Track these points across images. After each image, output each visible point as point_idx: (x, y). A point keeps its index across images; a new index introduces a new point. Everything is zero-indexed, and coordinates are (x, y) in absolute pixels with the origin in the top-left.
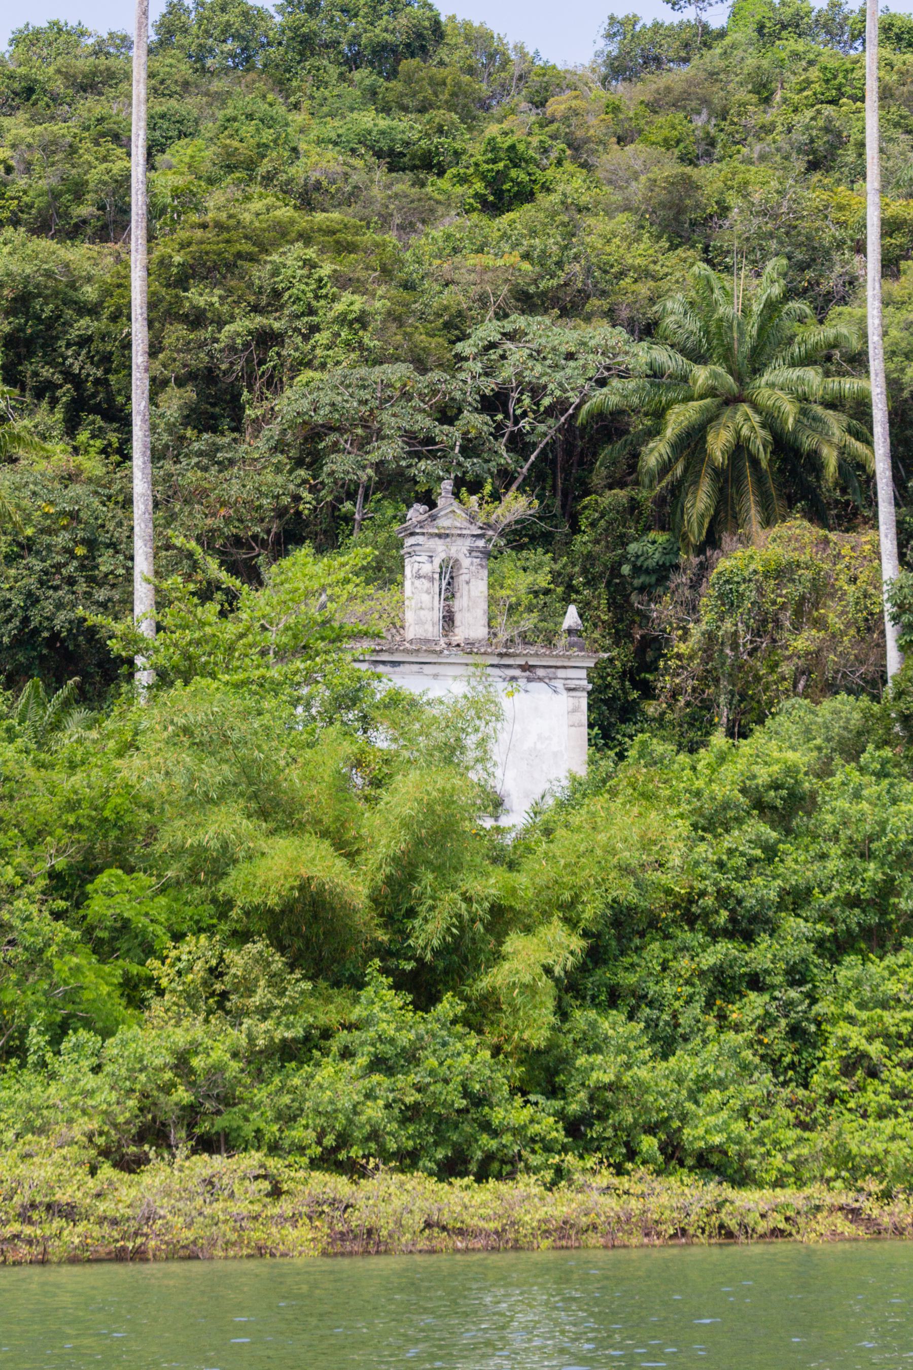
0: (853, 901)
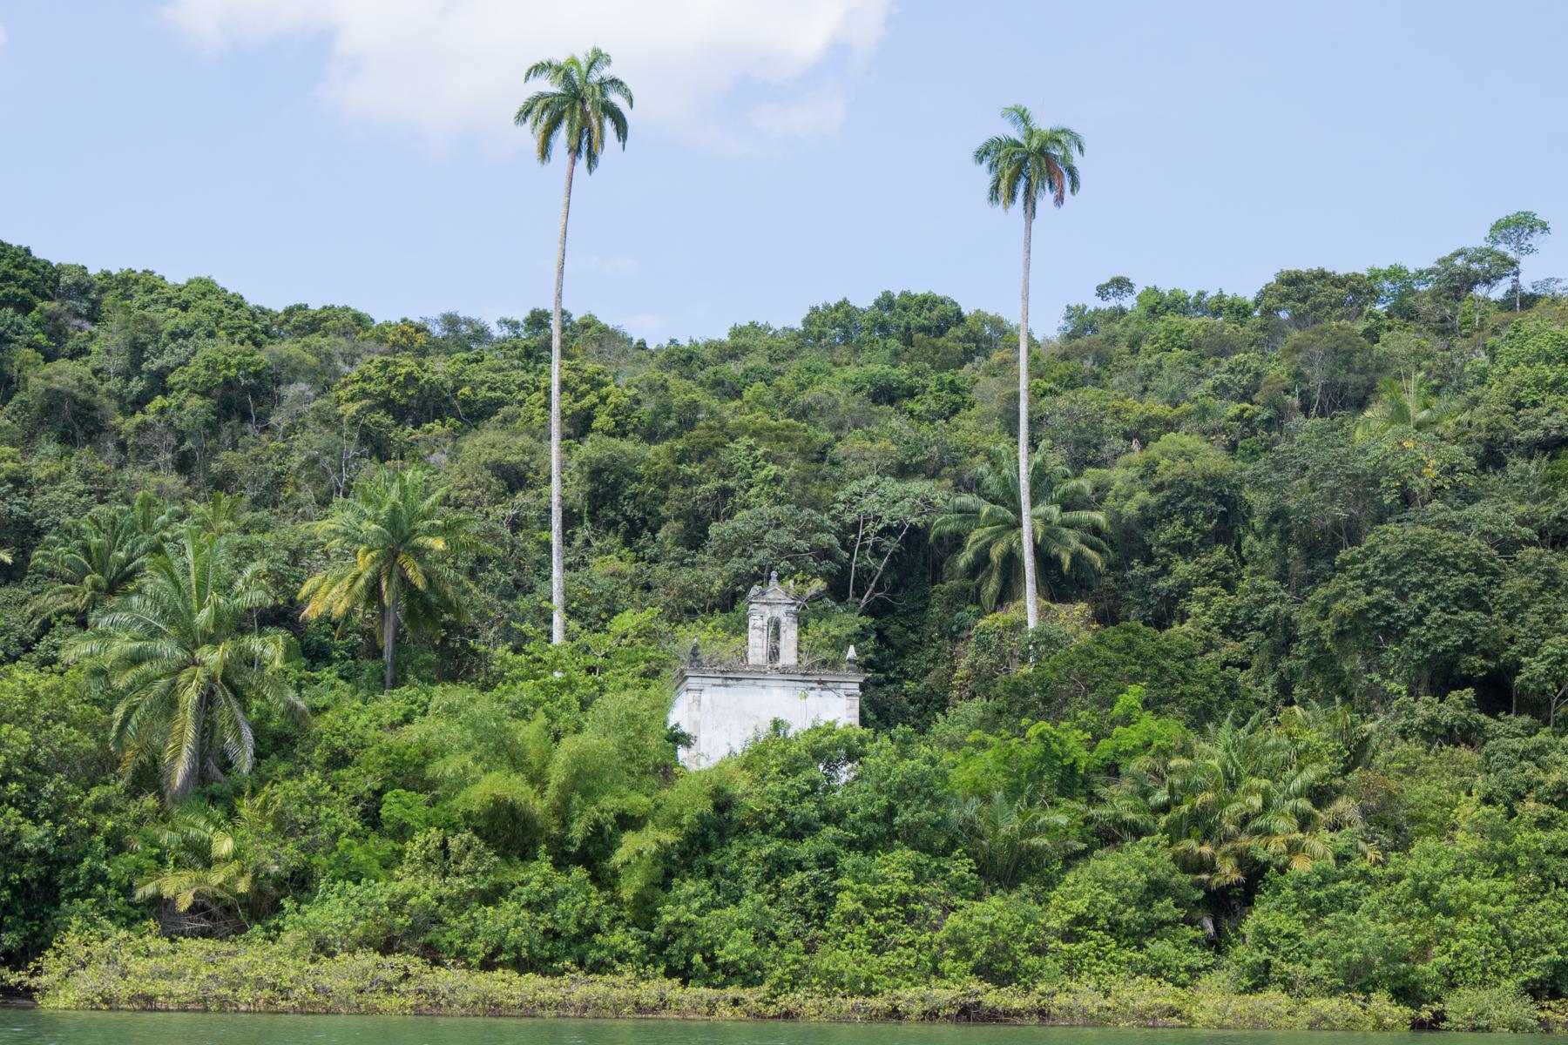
0: (872, 818)
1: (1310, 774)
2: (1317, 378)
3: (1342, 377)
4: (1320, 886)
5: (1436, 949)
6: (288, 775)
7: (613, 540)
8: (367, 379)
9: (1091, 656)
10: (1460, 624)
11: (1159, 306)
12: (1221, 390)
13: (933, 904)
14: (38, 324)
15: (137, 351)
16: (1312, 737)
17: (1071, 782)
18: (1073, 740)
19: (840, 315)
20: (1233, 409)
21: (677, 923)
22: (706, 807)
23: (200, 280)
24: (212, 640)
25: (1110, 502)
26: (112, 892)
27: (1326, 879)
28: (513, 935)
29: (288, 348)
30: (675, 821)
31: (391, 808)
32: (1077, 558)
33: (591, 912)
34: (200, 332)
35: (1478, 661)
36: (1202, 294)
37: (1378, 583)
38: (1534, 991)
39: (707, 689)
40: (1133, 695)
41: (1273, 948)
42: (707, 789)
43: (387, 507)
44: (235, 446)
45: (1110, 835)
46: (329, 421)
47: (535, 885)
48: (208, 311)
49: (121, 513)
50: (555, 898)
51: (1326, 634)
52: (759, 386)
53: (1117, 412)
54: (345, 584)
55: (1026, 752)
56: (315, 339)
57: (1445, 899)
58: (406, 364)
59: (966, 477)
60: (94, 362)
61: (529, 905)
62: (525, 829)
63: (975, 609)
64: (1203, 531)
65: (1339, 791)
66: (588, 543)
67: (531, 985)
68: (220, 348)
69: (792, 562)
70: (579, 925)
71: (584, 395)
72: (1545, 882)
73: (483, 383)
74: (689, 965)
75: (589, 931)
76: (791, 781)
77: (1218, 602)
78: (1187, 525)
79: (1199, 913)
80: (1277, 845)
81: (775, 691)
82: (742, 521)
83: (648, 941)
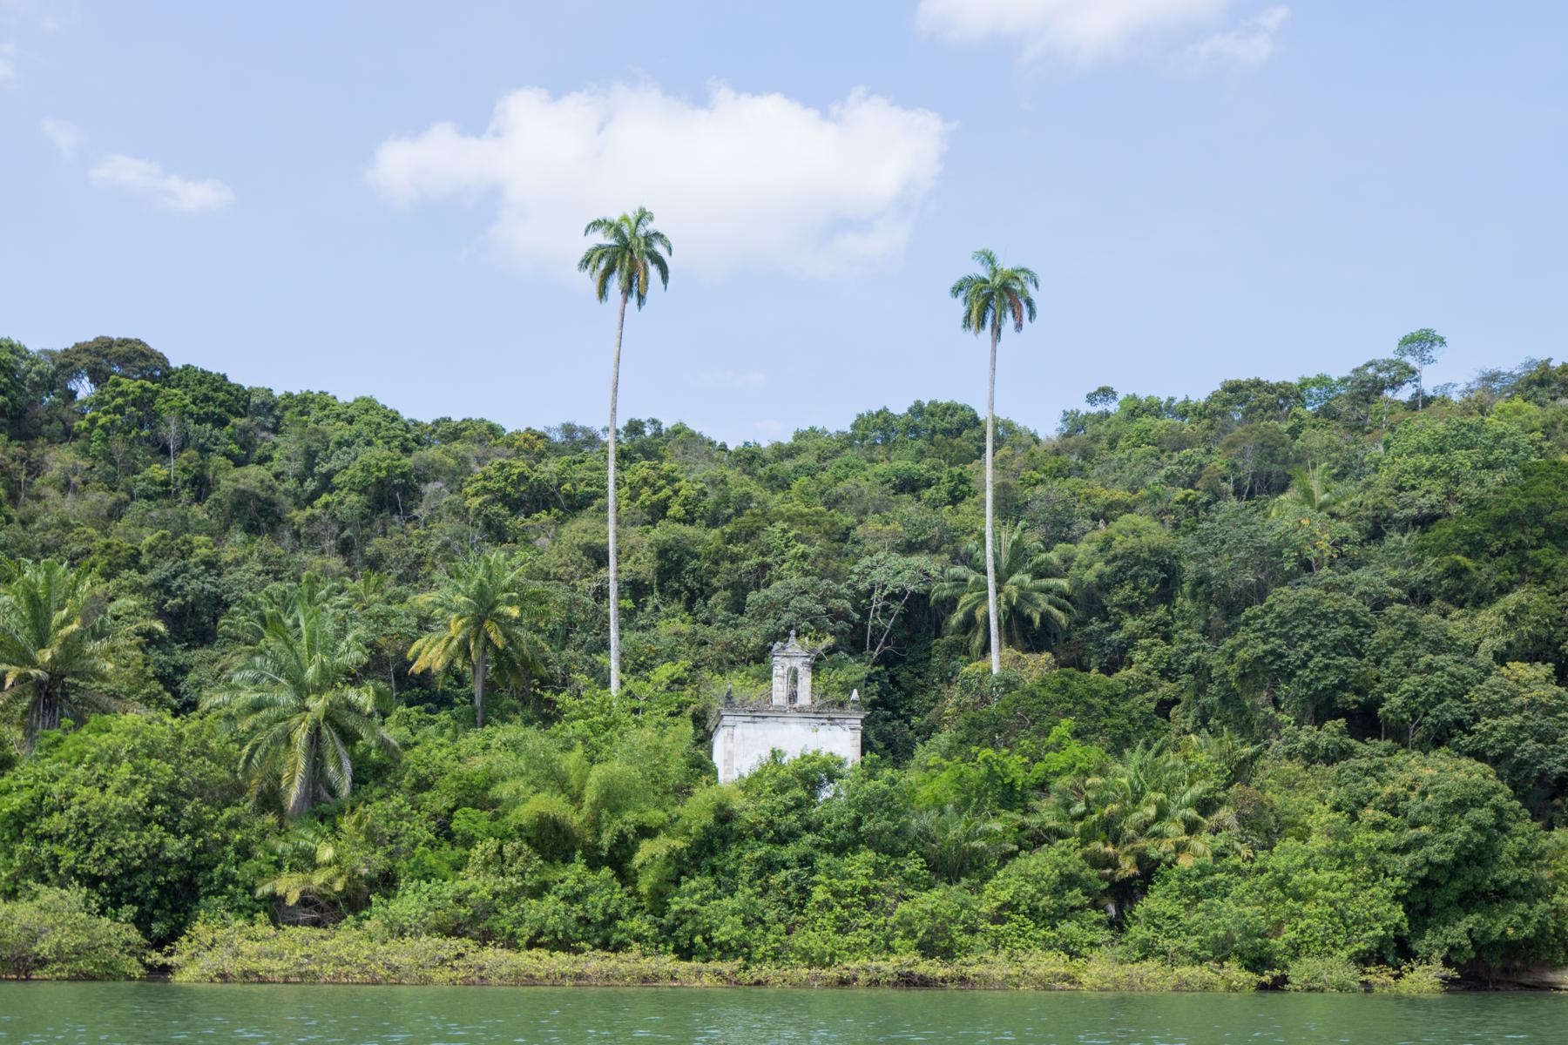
1: (1198, 789)
2: (1248, 467)
3: (1268, 467)
4: (1199, 877)
5: (1286, 927)
6: (382, 797)
7: (677, 606)
8: (487, 478)
9: (1033, 695)
10: (1337, 667)
11: (1137, 409)
12: (1171, 479)
13: (889, 894)
14: (231, 436)
15: (311, 457)
16: (1202, 759)
17: (1011, 797)
18: (1014, 765)
19: (880, 421)
20: (1180, 493)
21: (683, 911)
22: (709, 820)
23: (364, 399)
24: (319, 691)
25: (1074, 571)
26: (240, 890)
27: (1204, 872)
28: (551, 921)
29: (434, 453)
30: (685, 831)
31: (459, 823)
32: (1046, 616)
33: (614, 904)
34: (360, 441)
35: (1350, 697)
36: (1171, 400)
37: (1274, 635)
38: (1362, 960)
40: (1065, 726)
41: (1158, 927)
42: (711, 805)
43: (475, 582)
44: (385, 534)
45: (1037, 839)
46: (459, 512)
47: (570, 882)
48: (368, 424)
49: (291, 588)
50: (587, 891)
51: (1232, 677)
52: (804, 480)
53: (1088, 498)
54: (443, 644)
55: (973, 773)
56: (457, 446)
57: (1296, 887)
58: (520, 466)
59: (962, 552)
60: (276, 467)
61: (565, 898)
62: (566, 838)
63: (965, 658)
64: (1147, 594)
65: (1222, 802)
66: (657, 608)
67: (560, 961)
68: (378, 454)
69: (812, 623)
70: (604, 912)
71: (660, 489)
72: (1376, 873)
73: (582, 480)
74: (692, 945)
75: (611, 919)
76: (779, 799)
77: (1157, 651)
78: (1135, 589)
79: (1106, 900)
80: (1167, 846)
82: (775, 591)
83: (661, 926)
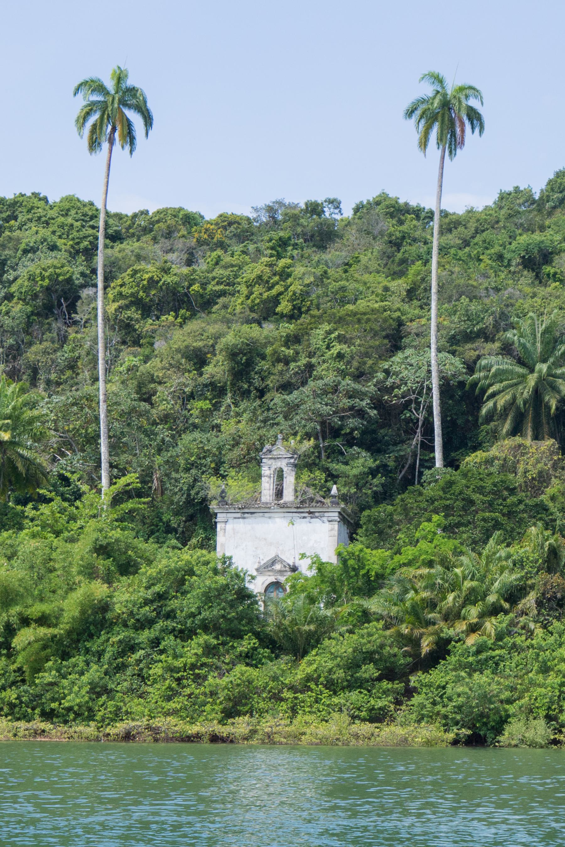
39: (231, 521)
81: (278, 520)
